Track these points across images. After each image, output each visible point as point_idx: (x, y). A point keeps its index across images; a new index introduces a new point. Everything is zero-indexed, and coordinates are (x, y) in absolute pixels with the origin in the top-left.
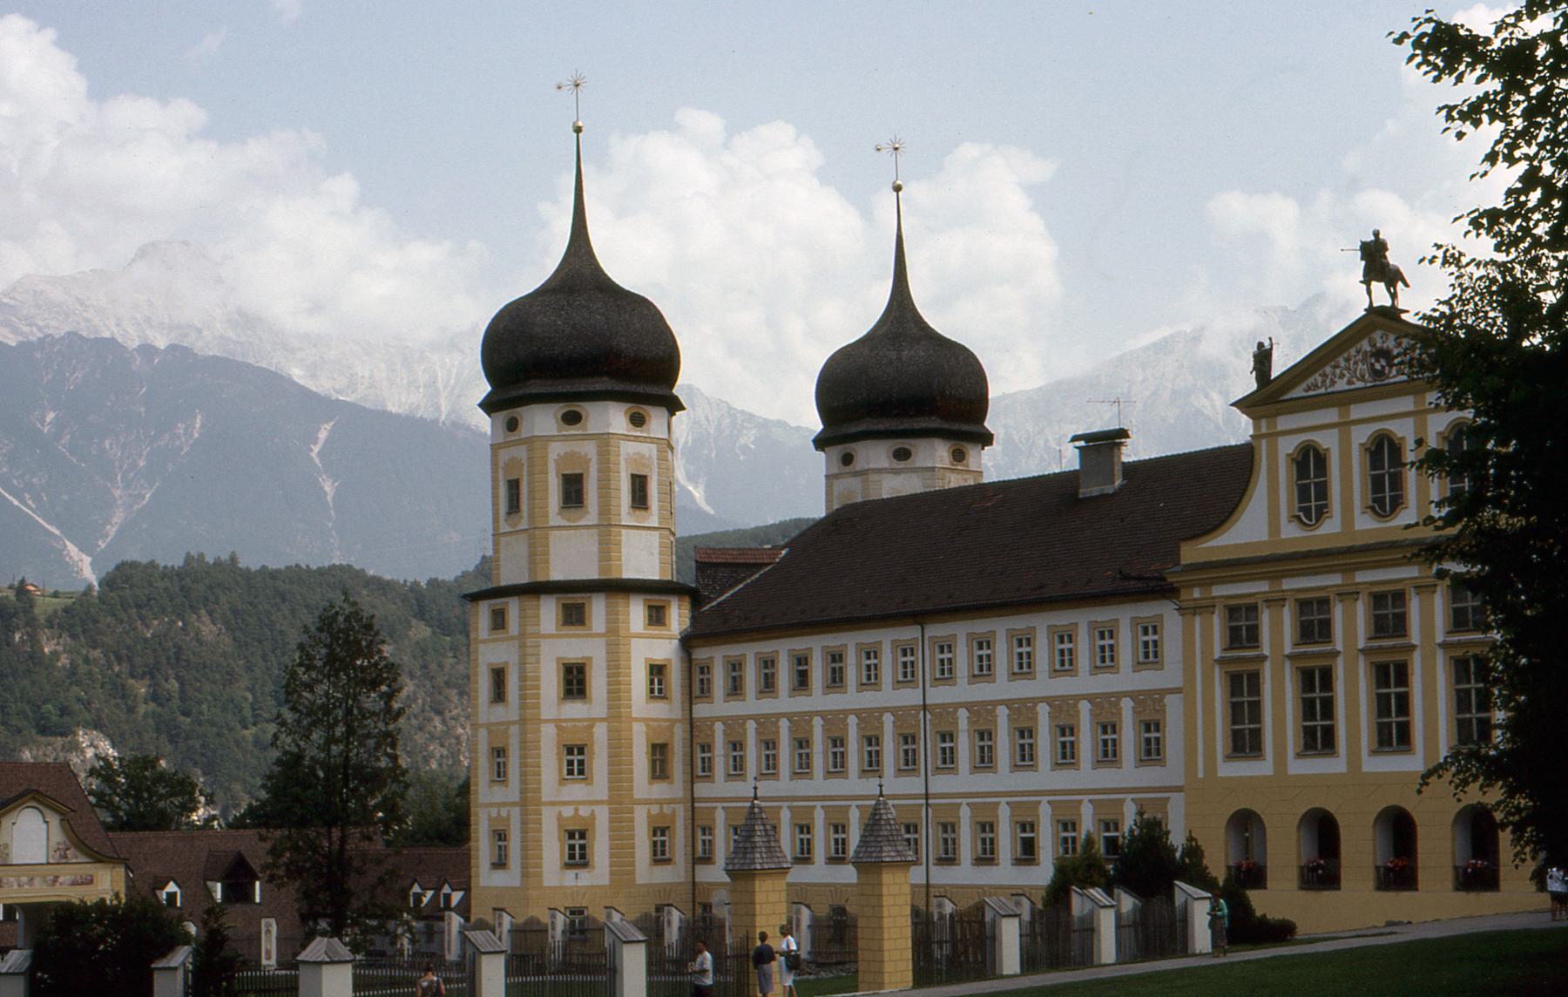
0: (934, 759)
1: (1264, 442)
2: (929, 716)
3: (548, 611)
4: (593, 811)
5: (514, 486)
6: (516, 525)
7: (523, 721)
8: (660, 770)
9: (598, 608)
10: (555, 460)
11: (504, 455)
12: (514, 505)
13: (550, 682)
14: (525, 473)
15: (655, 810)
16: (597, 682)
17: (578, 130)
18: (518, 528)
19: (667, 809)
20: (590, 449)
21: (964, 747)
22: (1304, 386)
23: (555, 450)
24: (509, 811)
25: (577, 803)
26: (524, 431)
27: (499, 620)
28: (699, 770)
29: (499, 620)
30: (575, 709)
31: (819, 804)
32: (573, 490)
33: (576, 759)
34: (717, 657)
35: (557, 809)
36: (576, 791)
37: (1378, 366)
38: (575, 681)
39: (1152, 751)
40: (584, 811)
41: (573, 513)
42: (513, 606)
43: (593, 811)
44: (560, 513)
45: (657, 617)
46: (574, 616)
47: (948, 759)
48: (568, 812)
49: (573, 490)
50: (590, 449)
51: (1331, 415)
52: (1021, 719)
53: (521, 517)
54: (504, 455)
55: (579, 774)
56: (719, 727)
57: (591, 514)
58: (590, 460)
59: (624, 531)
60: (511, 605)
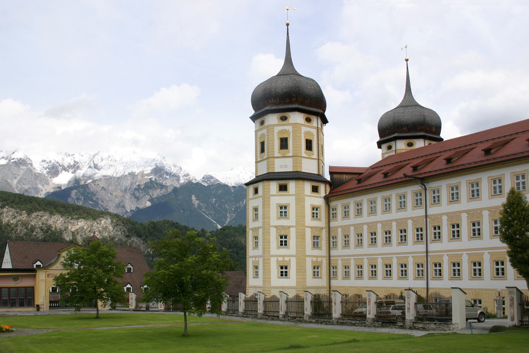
0: (431, 236)
2: (428, 220)
4: (290, 259)
5: (263, 144)
7: (263, 227)
8: (316, 245)
9: (292, 185)
10: (277, 132)
11: (260, 133)
12: (263, 150)
13: (274, 212)
14: (266, 138)
15: (315, 259)
16: (292, 211)
17: (288, 25)
18: (264, 159)
19: (319, 259)
20: (290, 128)
21: (446, 231)
23: (277, 129)
24: (259, 259)
25: (283, 256)
26: (266, 124)
27: (256, 191)
28: (331, 244)
29: (256, 191)
30: (283, 222)
31: (380, 257)
32: (284, 143)
33: (283, 242)
36: (283, 251)
38: (283, 210)
40: (287, 259)
43: (290, 259)
44: (279, 152)
45: (315, 189)
46: (283, 188)
47: (438, 236)
48: (281, 259)
49: (284, 143)
53: (265, 155)
54: (260, 133)
55: (285, 245)
56: (340, 230)
58: (290, 132)
59: (303, 159)
60: (259, 185)
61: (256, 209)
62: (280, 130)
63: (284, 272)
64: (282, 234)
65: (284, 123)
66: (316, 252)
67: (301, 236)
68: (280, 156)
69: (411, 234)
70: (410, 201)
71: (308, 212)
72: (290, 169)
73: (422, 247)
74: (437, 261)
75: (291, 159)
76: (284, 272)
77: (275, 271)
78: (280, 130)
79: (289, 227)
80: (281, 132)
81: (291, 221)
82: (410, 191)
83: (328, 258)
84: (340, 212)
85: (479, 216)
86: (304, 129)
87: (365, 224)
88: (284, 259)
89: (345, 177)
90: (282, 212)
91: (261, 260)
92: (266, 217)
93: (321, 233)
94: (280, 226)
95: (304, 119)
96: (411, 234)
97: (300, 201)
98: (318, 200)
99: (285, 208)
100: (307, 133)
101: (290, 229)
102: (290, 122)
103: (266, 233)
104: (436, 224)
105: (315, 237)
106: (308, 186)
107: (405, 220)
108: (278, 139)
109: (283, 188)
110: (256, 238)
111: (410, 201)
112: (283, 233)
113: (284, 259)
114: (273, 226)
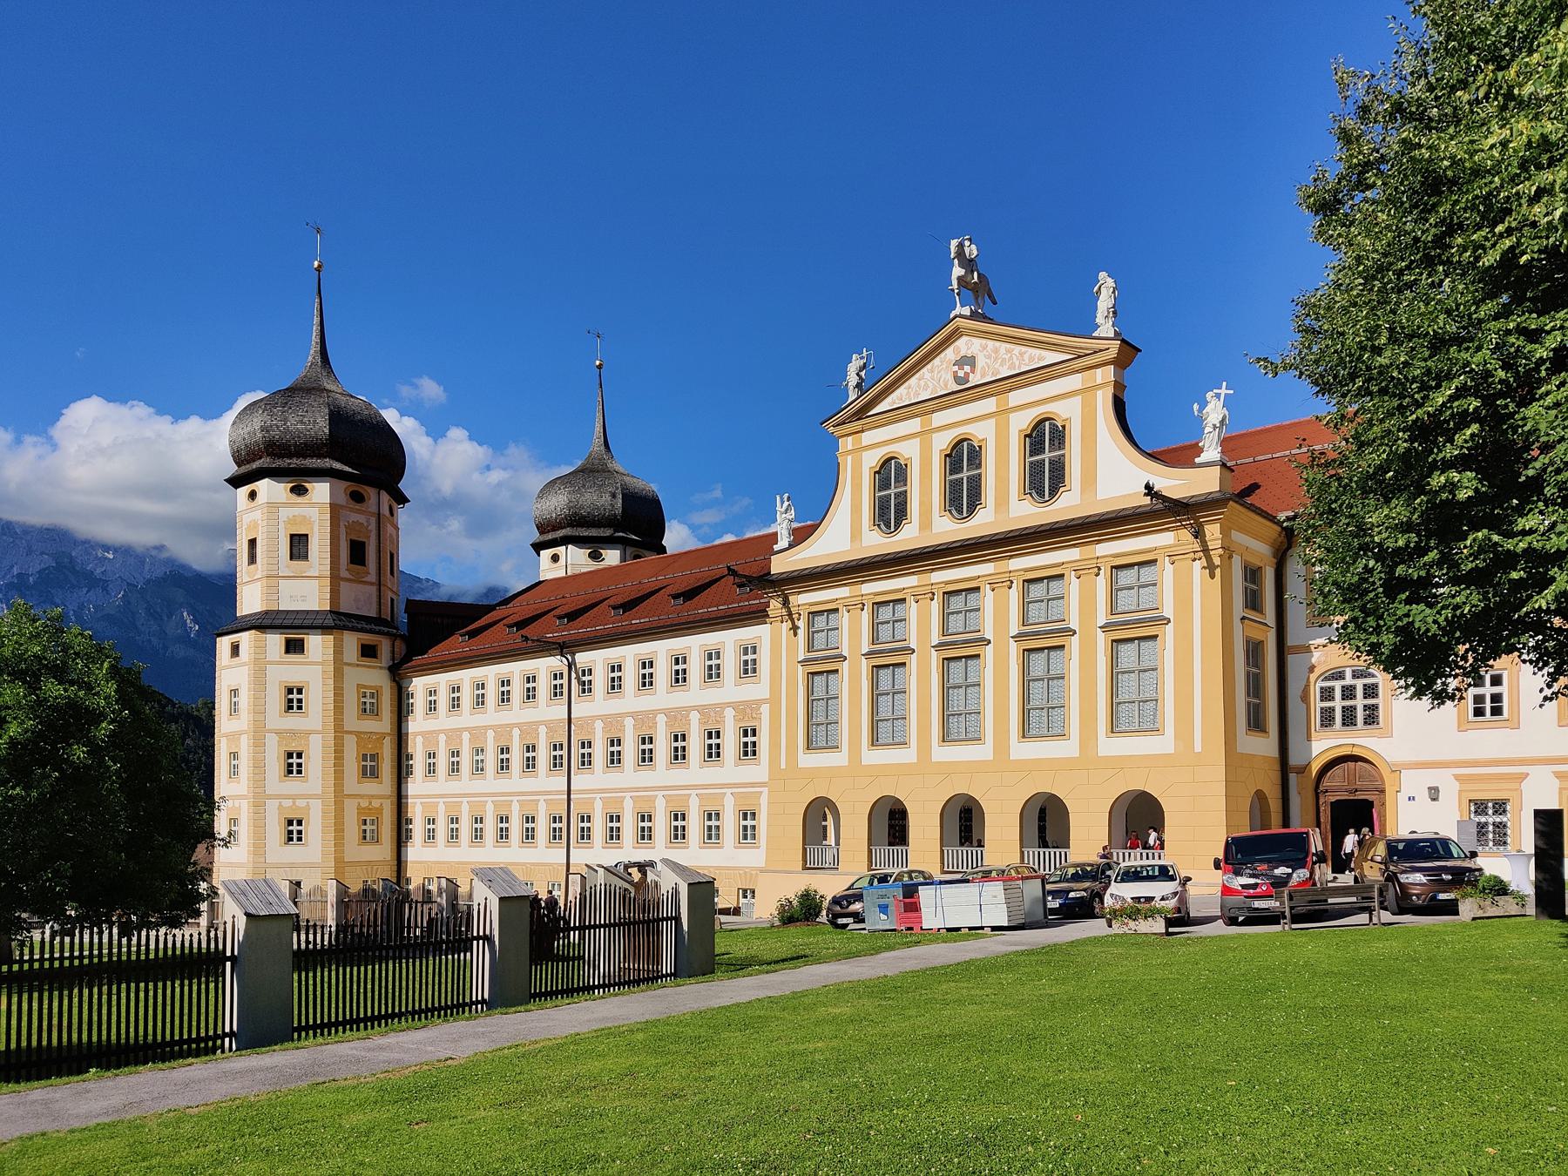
1: (849, 458)
4: (308, 802)
6: (254, 576)
15: (364, 803)
20: (313, 513)
22: (889, 400)
27: (235, 649)
29: (235, 649)
30: (294, 721)
35: (357, 801)
36: (293, 785)
37: (961, 373)
38: (293, 700)
39: (749, 751)
40: (301, 803)
41: (298, 565)
42: (246, 639)
43: (308, 802)
44: (287, 567)
46: (294, 647)
47: (586, 761)
48: (287, 803)
49: (298, 547)
51: (914, 425)
52: (644, 728)
62: (291, 517)
64: (290, 749)
65: (300, 500)
68: (292, 575)
74: (585, 811)
75: (315, 583)
78: (291, 517)
79: (309, 733)
80: (292, 521)
83: (395, 800)
84: (419, 701)
85: (651, 724)
87: (466, 729)
88: (294, 803)
90: (293, 699)
93: (382, 748)
94: (287, 731)
95: (346, 494)
99: (300, 691)
101: (310, 738)
102: (313, 501)
104: (586, 738)
108: (286, 537)
109: (294, 647)
110: (234, 755)
112: (294, 747)
113: (294, 803)
114: (270, 731)
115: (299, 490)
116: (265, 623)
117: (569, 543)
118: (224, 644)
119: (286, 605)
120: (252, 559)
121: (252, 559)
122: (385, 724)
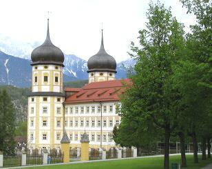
0: (103, 125)
3: (41, 98)
8: (58, 125)
9: (49, 98)
13: (41, 110)
20: (49, 72)
21: (108, 123)
27: (33, 100)
28: (65, 124)
29: (33, 100)
30: (45, 115)
32: (46, 78)
34: (68, 107)
36: (45, 128)
38: (45, 110)
42: (35, 98)
45: (59, 100)
46: (45, 99)
47: (105, 124)
49: (46, 78)
50: (49, 72)
57: (49, 83)
61: (33, 108)
63: (45, 137)
66: (59, 128)
67: (53, 121)
69: (96, 123)
70: (96, 109)
71: (56, 110)
72: (48, 91)
73: (99, 129)
76: (45, 137)
77: (41, 137)
80: (44, 74)
81: (48, 114)
82: (96, 106)
84: (69, 110)
86: (54, 72)
89: (71, 94)
91: (35, 132)
92: (37, 112)
96: (96, 123)
97: (53, 107)
98: (60, 105)
100: (56, 74)
103: (37, 120)
105: (58, 121)
106: (56, 99)
107: (94, 117)
109: (45, 99)
111: (96, 109)
115: (46, 67)
116: (39, 94)
117: (106, 82)
118: (30, 99)
119: (43, 91)
120: (36, 81)
121: (36, 81)
122: (61, 115)
